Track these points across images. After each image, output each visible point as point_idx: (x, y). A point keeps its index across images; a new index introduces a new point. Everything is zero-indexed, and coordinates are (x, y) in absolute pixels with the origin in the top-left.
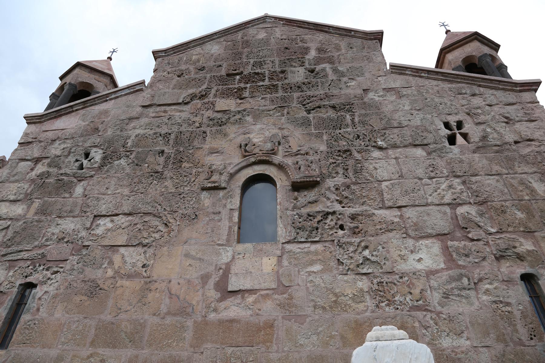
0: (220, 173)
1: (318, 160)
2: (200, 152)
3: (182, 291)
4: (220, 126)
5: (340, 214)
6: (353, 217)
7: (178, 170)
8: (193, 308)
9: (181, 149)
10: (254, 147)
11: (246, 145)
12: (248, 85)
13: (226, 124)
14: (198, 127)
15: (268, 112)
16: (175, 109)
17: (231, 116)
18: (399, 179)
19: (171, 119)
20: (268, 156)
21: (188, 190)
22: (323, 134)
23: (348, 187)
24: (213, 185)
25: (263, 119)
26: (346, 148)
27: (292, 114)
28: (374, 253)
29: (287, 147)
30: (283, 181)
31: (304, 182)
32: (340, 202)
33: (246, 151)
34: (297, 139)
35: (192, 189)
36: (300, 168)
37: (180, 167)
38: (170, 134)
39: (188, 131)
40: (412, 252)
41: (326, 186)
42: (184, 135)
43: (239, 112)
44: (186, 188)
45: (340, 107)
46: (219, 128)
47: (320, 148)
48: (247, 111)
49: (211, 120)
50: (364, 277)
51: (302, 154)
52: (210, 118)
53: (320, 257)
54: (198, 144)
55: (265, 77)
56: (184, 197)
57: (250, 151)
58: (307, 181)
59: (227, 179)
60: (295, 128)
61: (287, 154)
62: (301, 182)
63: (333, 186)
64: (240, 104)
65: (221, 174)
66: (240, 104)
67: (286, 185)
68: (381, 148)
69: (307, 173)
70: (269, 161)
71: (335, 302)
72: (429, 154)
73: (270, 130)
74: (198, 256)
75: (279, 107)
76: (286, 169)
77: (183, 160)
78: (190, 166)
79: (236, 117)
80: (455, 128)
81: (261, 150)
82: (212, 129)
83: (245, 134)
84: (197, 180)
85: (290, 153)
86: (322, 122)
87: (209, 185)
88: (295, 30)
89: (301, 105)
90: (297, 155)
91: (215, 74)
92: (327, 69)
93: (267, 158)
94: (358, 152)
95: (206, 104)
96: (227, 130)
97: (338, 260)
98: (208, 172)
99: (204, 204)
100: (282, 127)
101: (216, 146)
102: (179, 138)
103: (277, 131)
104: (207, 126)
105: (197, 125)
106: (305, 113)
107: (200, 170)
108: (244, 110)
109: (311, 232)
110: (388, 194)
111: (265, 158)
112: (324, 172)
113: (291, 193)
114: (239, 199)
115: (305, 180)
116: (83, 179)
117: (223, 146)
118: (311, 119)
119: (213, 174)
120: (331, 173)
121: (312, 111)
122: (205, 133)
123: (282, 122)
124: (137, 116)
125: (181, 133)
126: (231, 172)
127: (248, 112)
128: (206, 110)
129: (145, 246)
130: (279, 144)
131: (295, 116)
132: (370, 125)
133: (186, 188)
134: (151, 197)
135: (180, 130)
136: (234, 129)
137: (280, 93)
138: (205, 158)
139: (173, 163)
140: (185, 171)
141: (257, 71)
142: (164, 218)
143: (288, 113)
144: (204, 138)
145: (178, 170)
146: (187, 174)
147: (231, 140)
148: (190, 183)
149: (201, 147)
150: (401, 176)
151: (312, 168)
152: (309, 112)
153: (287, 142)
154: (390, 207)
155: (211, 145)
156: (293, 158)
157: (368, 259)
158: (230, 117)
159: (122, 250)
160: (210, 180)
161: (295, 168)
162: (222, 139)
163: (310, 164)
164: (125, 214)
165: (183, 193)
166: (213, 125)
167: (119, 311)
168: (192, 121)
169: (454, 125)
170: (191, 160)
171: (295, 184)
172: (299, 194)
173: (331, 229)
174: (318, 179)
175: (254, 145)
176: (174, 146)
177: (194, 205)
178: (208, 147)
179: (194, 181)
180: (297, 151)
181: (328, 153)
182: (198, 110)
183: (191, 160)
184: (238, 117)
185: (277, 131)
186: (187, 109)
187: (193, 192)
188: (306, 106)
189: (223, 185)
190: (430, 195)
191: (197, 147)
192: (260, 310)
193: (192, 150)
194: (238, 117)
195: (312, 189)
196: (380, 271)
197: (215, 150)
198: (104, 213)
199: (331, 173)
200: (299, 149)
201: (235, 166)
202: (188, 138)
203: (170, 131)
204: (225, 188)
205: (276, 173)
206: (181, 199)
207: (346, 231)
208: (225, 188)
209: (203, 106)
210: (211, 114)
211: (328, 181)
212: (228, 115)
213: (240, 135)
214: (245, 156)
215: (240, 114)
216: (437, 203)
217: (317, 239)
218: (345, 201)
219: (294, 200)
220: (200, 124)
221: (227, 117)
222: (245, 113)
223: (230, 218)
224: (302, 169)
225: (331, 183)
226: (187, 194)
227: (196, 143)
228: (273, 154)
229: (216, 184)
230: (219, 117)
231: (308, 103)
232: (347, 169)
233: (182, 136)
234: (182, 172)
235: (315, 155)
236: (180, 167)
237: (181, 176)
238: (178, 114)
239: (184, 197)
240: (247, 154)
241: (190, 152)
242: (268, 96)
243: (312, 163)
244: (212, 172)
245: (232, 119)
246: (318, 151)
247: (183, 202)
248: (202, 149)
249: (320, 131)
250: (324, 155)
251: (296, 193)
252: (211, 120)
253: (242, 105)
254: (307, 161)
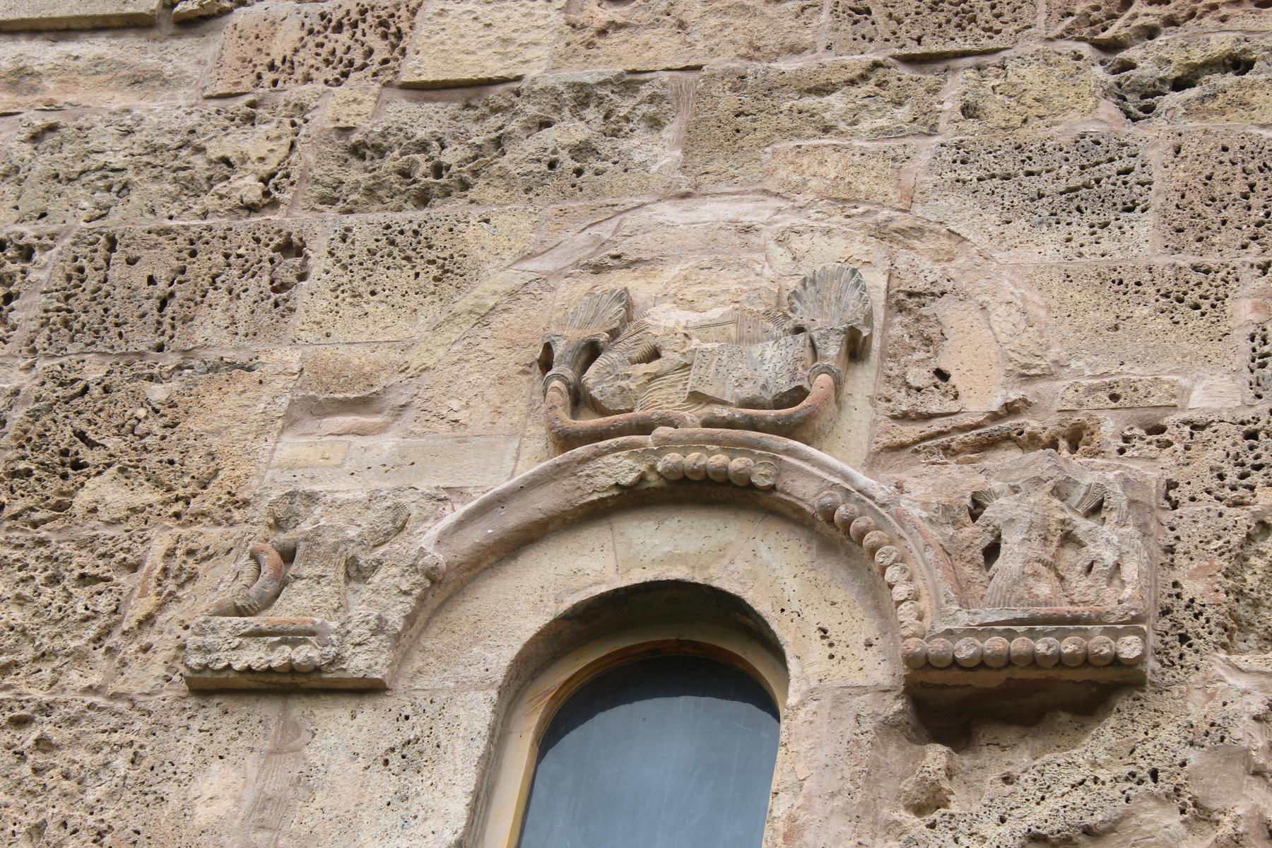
0: (352, 562)
1: (1153, 495)
2: (232, 400)
4: (423, 199)
7: (42, 533)
9: (93, 371)
10: (654, 366)
13: (465, 186)
14: (252, 208)
15: (810, 102)
16: (99, 61)
17: (514, 126)
19: (51, 139)
20: (747, 447)
21: (90, 690)
22: (1231, 277)
24: (278, 658)
25: (766, 154)
27: (998, 119)
29: (920, 376)
30: (839, 650)
31: (1009, 661)
33: (579, 399)
34: (1003, 319)
35: (119, 686)
36: (992, 552)
37: (60, 507)
39: (167, 231)
41: (1198, 710)
42: (131, 262)
43: (583, 96)
44: (74, 675)
46: (412, 216)
47: (1187, 392)
48: (645, 91)
49: (357, 151)
51: (1032, 442)
52: (355, 138)
56: (43, 744)
57: (610, 402)
58: (1033, 660)
59: (395, 618)
60: (1010, 231)
61: (910, 432)
62: (981, 663)
63: (1258, 706)
64: (602, 32)
65: (356, 572)
66: (602, 32)
67: (859, 680)
69: (1044, 589)
70: (751, 486)
73: (796, 243)
75: (909, 60)
76: (873, 550)
77: (87, 455)
78: (137, 501)
79: (549, 137)
81: (697, 398)
82: (350, 220)
83: (598, 269)
84: (173, 611)
85: (936, 425)
86: (1239, 186)
87: (254, 656)
89: (1085, 49)
90: (989, 444)
93: (737, 463)
95: (339, 28)
96: (472, 233)
98: (254, 556)
99: (185, 811)
100: (902, 221)
101: (359, 357)
102: (90, 285)
103: (857, 249)
104: (323, 200)
105: (247, 186)
106: (1108, 108)
107: (212, 535)
108: (628, 83)
111: (718, 459)
112: (1192, 588)
113: (894, 755)
114: (467, 780)
115: (1020, 645)
117: (415, 359)
118: (1156, 156)
119: (293, 570)
120: (1256, 604)
121: (1173, 99)
122: (299, 253)
123: (909, 180)
125: (112, 243)
126: (438, 557)
127: (652, 99)
128: (330, 74)
130: (856, 349)
131: (1023, 134)
133: (75, 678)
135: (113, 222)
136: (525, 224)
138: (263, 446)
139: (15, 474)
140: (88, 544)
143: (969, 111)
144: (284, 287)
145: (42, 533)
146: (102, 568)
147: (483, 318)
148: (115, 639)
149: (242, 358)
151: (1092, 550)
153: (928, 341)
155: (327, 353)
156: (953, 469)
158: (509, 137)
160: (253, 622)
162: (413, 300)
163: (1083, 526)
165: (46, 709)
166: (370, 192)
168: (214, 152)
170: (152, 460)
171: (936, 677)
172: (965, 761)
174: (1129, 648)
175: (655, 354)
176: (40, 341)
177: (108, 815)
178: (293, 358)
179: (148, 620)
180: (995, 417)
181: (1252, 435)
182: (268, 77)
183: (152, 460)
184: (570, 131)
185: (857, 249)
186: (189, 68)
187: (121, 706)
188: (1124, 55)
189: (358, 664)
191: (212, 356)
193: (175, 385)
194: (570, 131)
195: (1082, 729)
197: (350, 384)
199: (1256, 604)
200: (1013, 396)
201: (484, 510)
202: (162, 287)
203: (29, 231)
204: (369, 689)
205: (791, 585)
206: (21, 756)
208: (369, 689)
209: (311, 41)
210: (368, 107)
211: (1219, 670)
212: (495, 121)
213: (560, 274)
214: (566, 440)
215: (591, 113)
219: (919, 810)
220: (264, 181)
221: (480, 134)
222: (624, 106)
224: (1009, 560)
225: (1242, 682)
226: (73, 721)
228: (788, 429)
229: (303, 654)
230: (421, 134)
231: (1150, 33)
233: (118, 271)
234: (68, 548)
235: (1142, 447)
236: (60, 507)
237: (54, 580)
238: (120, 99)
239: (43, 744)
240: (589, 422)
241: (158, 393)
243: (1096, 510)
244: (288, 555)
245: (519, 156)
246: (1169, 420)
247: (31, 782)
248: (247, 378)
249: (1211, 260)
250: (1213, 456)
251: (936, 756)
252: (357, 151)
253: (615, 37)
254: (1057, 492)
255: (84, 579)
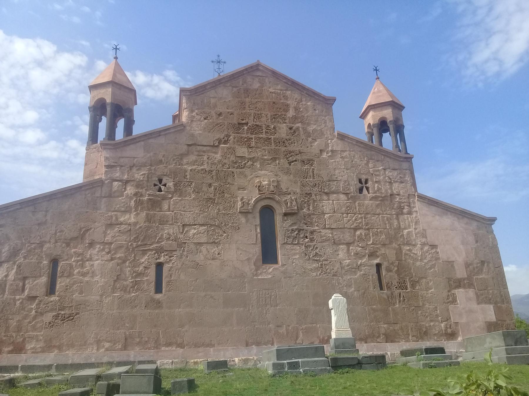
3: (240, 266)
5: (306, 231)
6: (312, 233)
8: (246, 274)
11: (259, 186)
12: (253, 136)
18: (334, 213)
23: (310, 216)
26: (309, 192)
28: (320, 251)
32: (306, 224)
36: (287, 203)
38: (212, 171)
40: (335, 251)
45: (307, 162)
50: (316, 261)
53: (298, 252)
54: (231, 181)
55: (262, 130)
68: (327, 194)
71: (304, 272)
72: (348, 199)
74: (244, 249)
80: (364, 183)
87: (244, 211)
88: (279, 83)
91: (230, 122)
92: (300, 129)
94: (315, 195)
97: (305, 253)
109: (294, 239)
110: (328, 221)
116: (164, 198)
124: (186, 153)
129: (217, 243)
132: (322, 177)
134: (212, 215)
137: (273, 146)
141: (257, 124)
142: (223, 228)
150: (334, 212)
152: (290, 163)
154: (328, 228)
157: (317, 253)
159: (205, 246)
161: (285, 204)
164: (200, 225)
167: (213, 276)
169: (363, 181)
173: (302, 238)
189: (251, 211)
190: (346, 223)
192: (274, 274)
196: (322, 259)
198: (188, 223)
207: (308, 239)
210: (234, 158)
216: (349, 227)
217: (296, 243)
218: (308, 223)
223: (256, 230)
227: (229, 180)
229: (247, 211)
232: (310, 205)
242: (266, 148)
255: (228, 203)
